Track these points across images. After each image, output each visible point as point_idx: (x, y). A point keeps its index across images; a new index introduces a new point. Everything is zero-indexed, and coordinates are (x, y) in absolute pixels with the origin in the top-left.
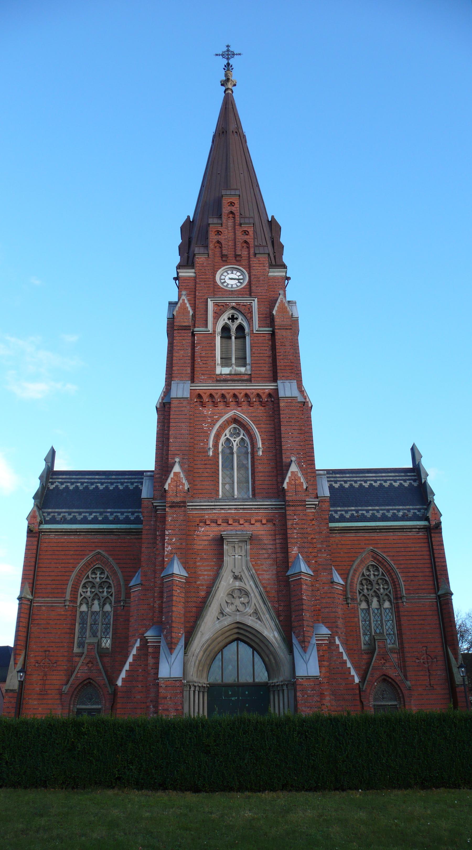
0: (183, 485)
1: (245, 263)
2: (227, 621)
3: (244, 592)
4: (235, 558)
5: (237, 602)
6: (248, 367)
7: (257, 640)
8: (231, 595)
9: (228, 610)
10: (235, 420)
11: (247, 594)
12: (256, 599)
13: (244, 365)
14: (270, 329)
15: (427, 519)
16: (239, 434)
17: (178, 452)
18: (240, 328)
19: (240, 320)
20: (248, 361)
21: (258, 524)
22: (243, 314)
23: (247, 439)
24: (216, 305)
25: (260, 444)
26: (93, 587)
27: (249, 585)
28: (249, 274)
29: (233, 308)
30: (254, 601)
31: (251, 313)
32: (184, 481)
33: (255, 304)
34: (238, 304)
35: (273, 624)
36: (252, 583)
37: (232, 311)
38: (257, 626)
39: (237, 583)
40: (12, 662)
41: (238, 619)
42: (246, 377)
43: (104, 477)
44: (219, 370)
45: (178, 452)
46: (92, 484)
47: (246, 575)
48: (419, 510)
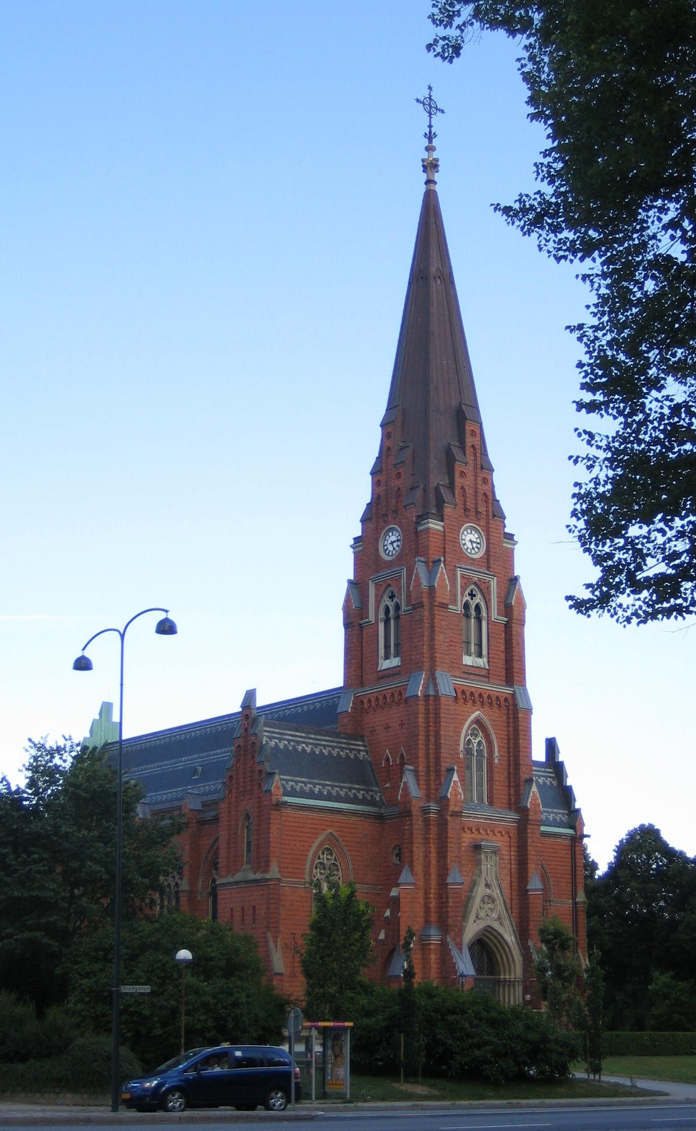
0: (460, 794)
1: (483, 523)
2: (481, 925)
3: (491, 899)
4: (490, 868)
5: (486, 907)
6: (485, 659)
7: (496, 942)
8: (483, 901)
9: (482, 914)
10: (478, 721)
11: (493, 901)
12: (500, 906)
13: (480, 655)
14: (506, 619)
15: (573, 827)
16: (476, 735)
17: (448, 756)
18: (478, 607)
19: (478, 599)
20: (485, 652)
21: (499, 835)
22: (483, 594)
23: (484, 742)
24: (463, 576)
25: (496, 754)
26: (325, 868)
27: (496, 893)
28: (488, 539)
29: (475, 583)
30: (499, 908)
31: (489, 593)
32: (460, 790)
33: (494, 583)
34: (480, 580)
35: (511, 929)
36: (498, 891)
37: (473, 587)
38: (501, 930)
39: (488, 891)
40: (272, 945)
41: (489, 923)
42: (484, 673)
43: (303, 735)
44: (468, 660)
45: (448, 756)
46: (298, 743)
47: (494, 883)
48: (563, 814)
